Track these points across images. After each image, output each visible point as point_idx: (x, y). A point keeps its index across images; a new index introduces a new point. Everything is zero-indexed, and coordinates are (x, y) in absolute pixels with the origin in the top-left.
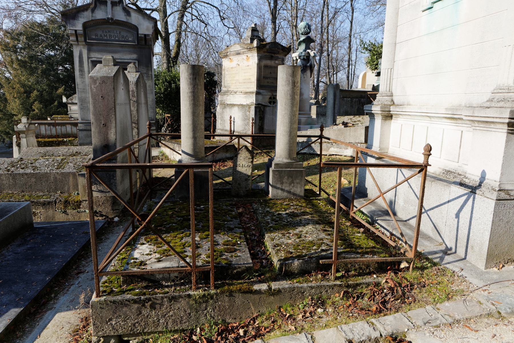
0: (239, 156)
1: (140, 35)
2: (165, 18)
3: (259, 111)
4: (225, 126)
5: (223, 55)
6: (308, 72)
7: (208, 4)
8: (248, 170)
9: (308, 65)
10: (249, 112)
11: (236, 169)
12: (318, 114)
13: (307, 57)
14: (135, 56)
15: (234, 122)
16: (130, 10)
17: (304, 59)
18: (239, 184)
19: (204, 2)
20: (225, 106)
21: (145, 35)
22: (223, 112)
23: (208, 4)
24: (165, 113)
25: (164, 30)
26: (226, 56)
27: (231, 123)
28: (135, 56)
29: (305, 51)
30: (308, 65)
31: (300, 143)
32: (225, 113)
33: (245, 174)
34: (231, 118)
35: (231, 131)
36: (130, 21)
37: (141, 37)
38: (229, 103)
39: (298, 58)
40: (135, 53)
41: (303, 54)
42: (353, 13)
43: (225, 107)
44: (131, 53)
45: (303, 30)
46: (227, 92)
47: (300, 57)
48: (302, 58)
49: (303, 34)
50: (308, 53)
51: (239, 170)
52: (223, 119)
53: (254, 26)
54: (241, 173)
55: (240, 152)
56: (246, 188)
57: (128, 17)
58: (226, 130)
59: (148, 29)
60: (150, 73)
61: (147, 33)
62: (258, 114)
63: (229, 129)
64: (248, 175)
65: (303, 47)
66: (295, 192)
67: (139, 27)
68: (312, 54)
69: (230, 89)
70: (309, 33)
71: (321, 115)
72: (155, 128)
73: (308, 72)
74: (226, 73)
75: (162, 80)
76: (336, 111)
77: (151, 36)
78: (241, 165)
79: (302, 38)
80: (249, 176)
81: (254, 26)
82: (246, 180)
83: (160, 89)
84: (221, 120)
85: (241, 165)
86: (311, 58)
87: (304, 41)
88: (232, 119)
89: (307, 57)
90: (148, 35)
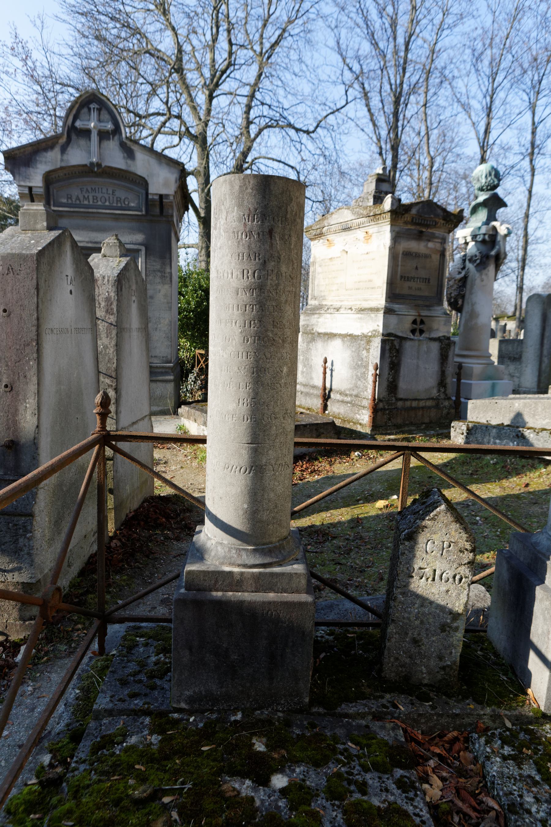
0: (422, 538)
1: (150, 197)
2: (206, 186)
3: (390, 349)
4: (312, 378)
5: (314, 233)
6: (491, 268)
7: (280, 161)
9: (493, 253)
10: (368, 350)
11: (407, 585)
12: (501, 357)
13: (490, 236)
14: (139, 237)
15: (332, 370)
16: (135, 148)
17: (484, 242)
18: (416, 642)
19: (273, 160)
20: (315, 336)
21: (161, 196)
22: (308, 350)
23: (280, 161)
24: (195, 348)
25: (203, 206)
26: (320, 235)
27: (325, 373)
28: (139, 237)
29: (487, 223)
30: (493, 253)
31: (494, 427)
32: (313, 352)
33: (442, 608)
34: (325, 361)
35: (325, 388)
36: (132, 169)
37: (153, 200)
38: (321, 330)
39: (469, 239)
40: (140, 231)
41: (483, 230)
42: (533, 175)
43: (313, 340)
44: (133, 230)
45: (483, 181)
46: (320, 307)
47: (474, 237)
48: (480, 238)
49: (481, 189)
50: (494, 228)
51: (420, 591)
52: (309, 366)
53: (381, 172)
54: (424, 601)
55: (426, 522)
56: (441, 658)
57: (129, 162)
58: (314, 387)
59: (166, 184)
60: (168, 270)
61: (163, 192)
62: (387, 355)
63: (320, 384)
64: (451, 612)
65: (482, 215)
67: (150, 181)
68: (502, 230)
69: (324, 303)
70: (495, 187)
71: (510, 358)
72: (172, 377)
73: (491, 268)
74: (319, 269)
75: (194, 285)
76: (545, 352)
77: (172, 198)
78: (428, 571)
79: (483, 197)
80: (456, 616)
81: (381, 172)
82: (444, 628)
83: (188, 303)
84: (305, 366)
85: (428, 571)
86: (499, 238)
87: (485, 204)
88: (329, 364)
89: (490, 236)
90: (167, 196)
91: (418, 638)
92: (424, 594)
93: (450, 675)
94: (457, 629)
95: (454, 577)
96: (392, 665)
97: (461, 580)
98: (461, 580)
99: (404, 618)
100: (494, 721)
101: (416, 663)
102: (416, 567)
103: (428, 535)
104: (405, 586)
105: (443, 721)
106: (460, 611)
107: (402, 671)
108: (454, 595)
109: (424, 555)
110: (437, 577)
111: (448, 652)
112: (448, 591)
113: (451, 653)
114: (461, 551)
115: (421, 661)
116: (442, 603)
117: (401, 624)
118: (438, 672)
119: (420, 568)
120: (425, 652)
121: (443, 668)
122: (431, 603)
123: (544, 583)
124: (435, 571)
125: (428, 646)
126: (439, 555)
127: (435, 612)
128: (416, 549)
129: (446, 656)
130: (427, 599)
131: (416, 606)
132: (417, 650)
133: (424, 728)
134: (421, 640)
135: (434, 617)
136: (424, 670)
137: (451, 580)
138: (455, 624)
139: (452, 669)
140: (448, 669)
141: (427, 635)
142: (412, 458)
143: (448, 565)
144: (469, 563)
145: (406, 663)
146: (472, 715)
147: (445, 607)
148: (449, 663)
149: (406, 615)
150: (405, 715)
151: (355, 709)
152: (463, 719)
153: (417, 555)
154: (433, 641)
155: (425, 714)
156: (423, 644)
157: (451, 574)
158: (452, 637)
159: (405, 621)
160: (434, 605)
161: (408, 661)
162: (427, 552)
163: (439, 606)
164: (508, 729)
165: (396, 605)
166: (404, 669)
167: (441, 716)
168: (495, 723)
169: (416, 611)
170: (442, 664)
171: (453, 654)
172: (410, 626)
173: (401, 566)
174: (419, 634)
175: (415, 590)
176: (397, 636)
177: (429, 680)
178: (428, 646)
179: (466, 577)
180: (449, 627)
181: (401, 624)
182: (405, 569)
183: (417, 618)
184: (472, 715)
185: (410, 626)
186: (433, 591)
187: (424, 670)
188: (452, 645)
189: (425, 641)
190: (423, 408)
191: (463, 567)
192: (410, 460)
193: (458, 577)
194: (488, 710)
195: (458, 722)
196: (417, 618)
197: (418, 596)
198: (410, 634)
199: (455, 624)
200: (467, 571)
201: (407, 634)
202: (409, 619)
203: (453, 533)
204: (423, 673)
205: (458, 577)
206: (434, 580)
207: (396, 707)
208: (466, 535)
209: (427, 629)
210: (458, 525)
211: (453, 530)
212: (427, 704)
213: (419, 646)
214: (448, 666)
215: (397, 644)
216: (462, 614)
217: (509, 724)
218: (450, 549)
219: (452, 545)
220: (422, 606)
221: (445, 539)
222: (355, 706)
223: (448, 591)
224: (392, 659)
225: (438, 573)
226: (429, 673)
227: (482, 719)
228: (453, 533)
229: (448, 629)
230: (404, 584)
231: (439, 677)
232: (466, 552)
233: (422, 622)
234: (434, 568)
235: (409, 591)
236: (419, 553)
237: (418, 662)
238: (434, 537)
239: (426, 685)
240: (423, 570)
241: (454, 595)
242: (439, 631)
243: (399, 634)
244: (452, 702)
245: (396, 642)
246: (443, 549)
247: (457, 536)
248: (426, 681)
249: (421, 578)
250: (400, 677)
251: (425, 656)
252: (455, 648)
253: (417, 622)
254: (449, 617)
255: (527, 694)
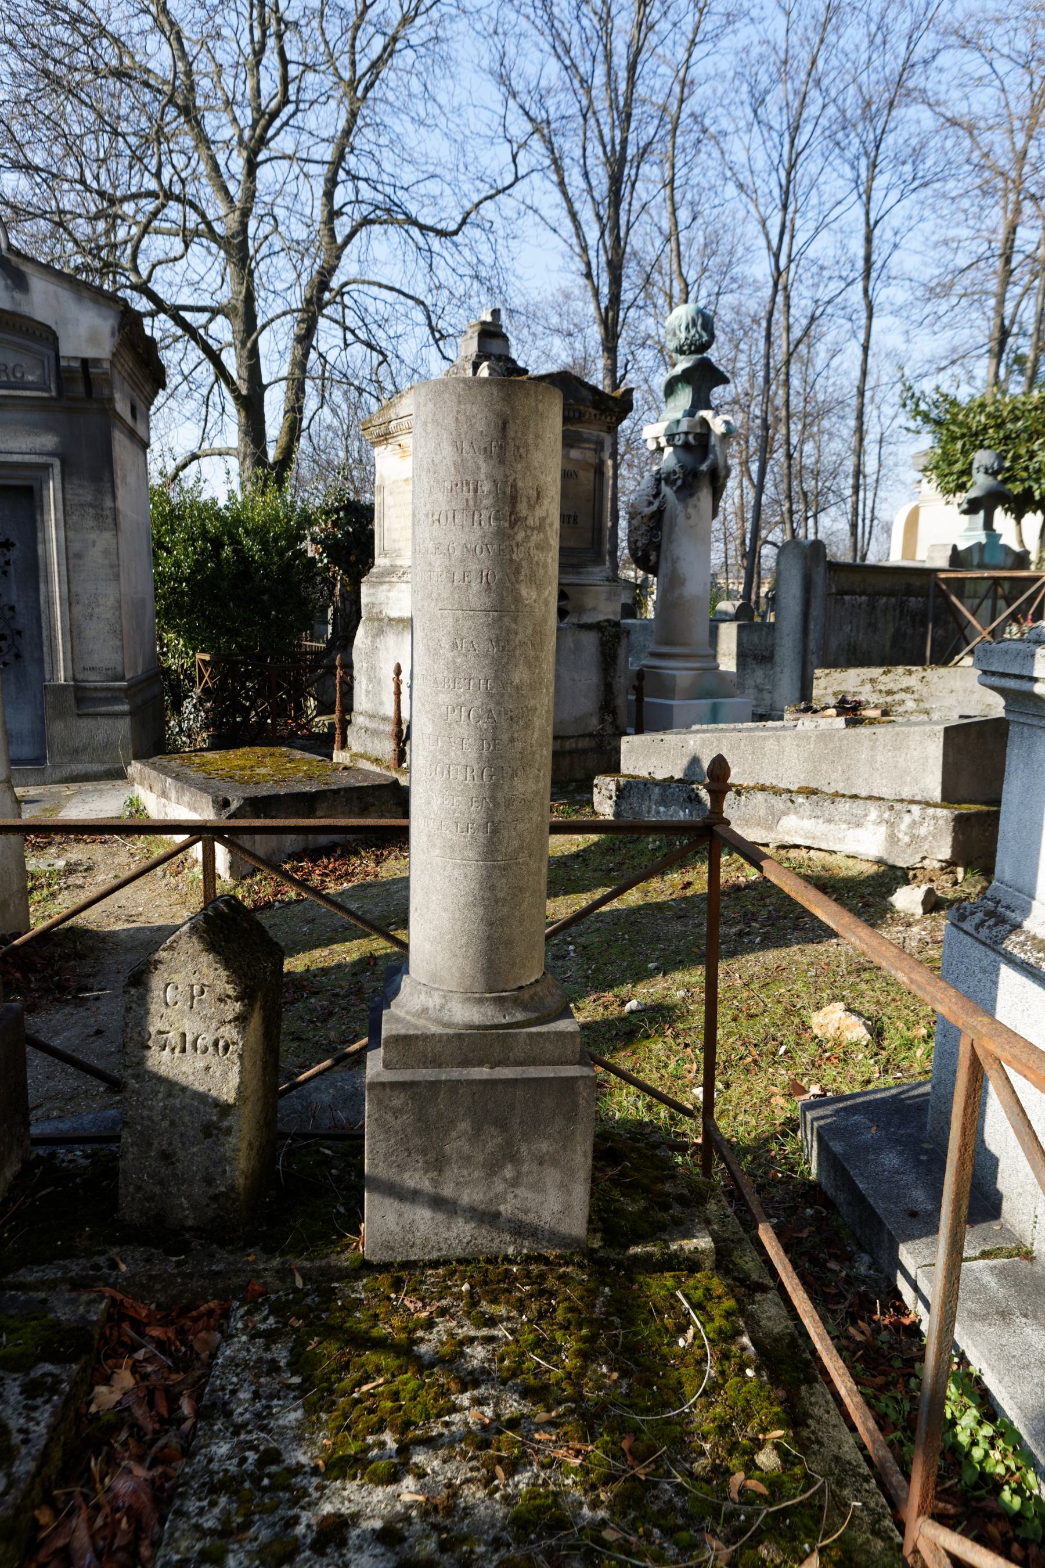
0: (157, 981)
1: (63, 363)
2: (249, 336)
4: (381, 703)
5: (376, 431)
6: (705, 496)
7: (392, 289)
8: (217, 1071)
9: (704, 467)
11: (142, 1061)
12: (743, 656)
13: (697, 436)
14: (48, 441)
15: (411, 687)
16: (27, 268)
17: (686, 446)
18: (166, 1157)
19: (380, 285)
20: (387, 624)
21: (85, 362)
22: (375, 649)
23: (392, 289)
24: (194, 650)
25: (245, 374)
26: (385, 437)
27: (398, 693)
28: (48, 441)
29: (691, 413)
30: (704, 467)
31: (656, 783)
32: (382, 654)
33: (202, 1098)
34: (398, 671)
35: (399, 721)
36: (25, 310)
37: (69, 369)
38: (394, 614)
39: (663, 442)
40: (49, 428)
41: (684, 427)
42: (870, 317)
43: (381, 632)
44: (34, 428)
45: (683, 335)
46: (391, 571)
47: (671, 437)
48: (679, 441)
49: (680, 351)
50: (704, 422)
51: (163, 1071)
52: (374, 678)
53: (489, 319)
54: (172, 1087)
55: (162, 955)
56: (209, 1181)
57: (18, 296)
58: (385, 719)
59: (93, 339)
60: (108, 503)
61: (90, 353)
63: (390, 711)
64: (216, 1103)
65: (684, 397)
66: (530, 1218)
67: (60, 333)
68: (718, 426)
69: (399, 563)
70: (704, 347)
71: (755, 657)
72: (126, 708)
73: (705, 496)
74: (389, 500)
75: (187, 530)
76: (812, 645)
77: (106, 365)
78: (173, 1037)
79: (684, 364)
80: (224, 1109)
81: (489, 319)
82: (209, 1130)
83: (177, 564)
84: (370, 680)
85: (173, 1037)
86: (713, 440)
87: (686, 377)
88: (405, 677)
89: (697, 436)
90: (97, 361)
94: (229, 1131)
95: (216, 1044)
97: (226, 1048)
98: (226, 1048)
102: (153, 1030)
106: (231, 1101)
109: (163, 1010)
110: (188, 1046)
114: (221, 1000)
116: (201, 1089)
119: (161, 1033)
121: (215, 1198)
122: (184, 1089)
124: (184, 1035)
126: (186, 1008)
130: (176, 1084)
135: (191, 1114)
137: (211, 1049)
138: (226, 1124)
144: (236, 1019)
149: (146, 1113)
150: (126, 1279)
159: (147, 1123)
161: (157, 1189)
167: (190, 1276)
170: (212, 1191)
174: (170, 1144)
175: (155, 1069)
176: (135, 1149)
182: (136, 1036)
183: (164, 1117)
188: (224, 1159)
189: (181, 1154)
190: (571, 752)
193: (221, 1043)
195: (220, 1286)
196: (164, 1117)
199: (226, 1124)
200: (234, 1033)
201: (150, 1145)
202: (150, 1118)
203: (205, 970)
209: (182, 1135)
214: (222, 1194)
223: (207, 1068)
224: (131, 1189)
225: (189, 1038)
228: (205, 970)
233: (172, 1123)
236: (155, 1007)
237: (174, 1190)
238: (176, 978)
239: (190, 1229)
247: (212, 974)
248: (190, 1222)
253: (165, 1124)
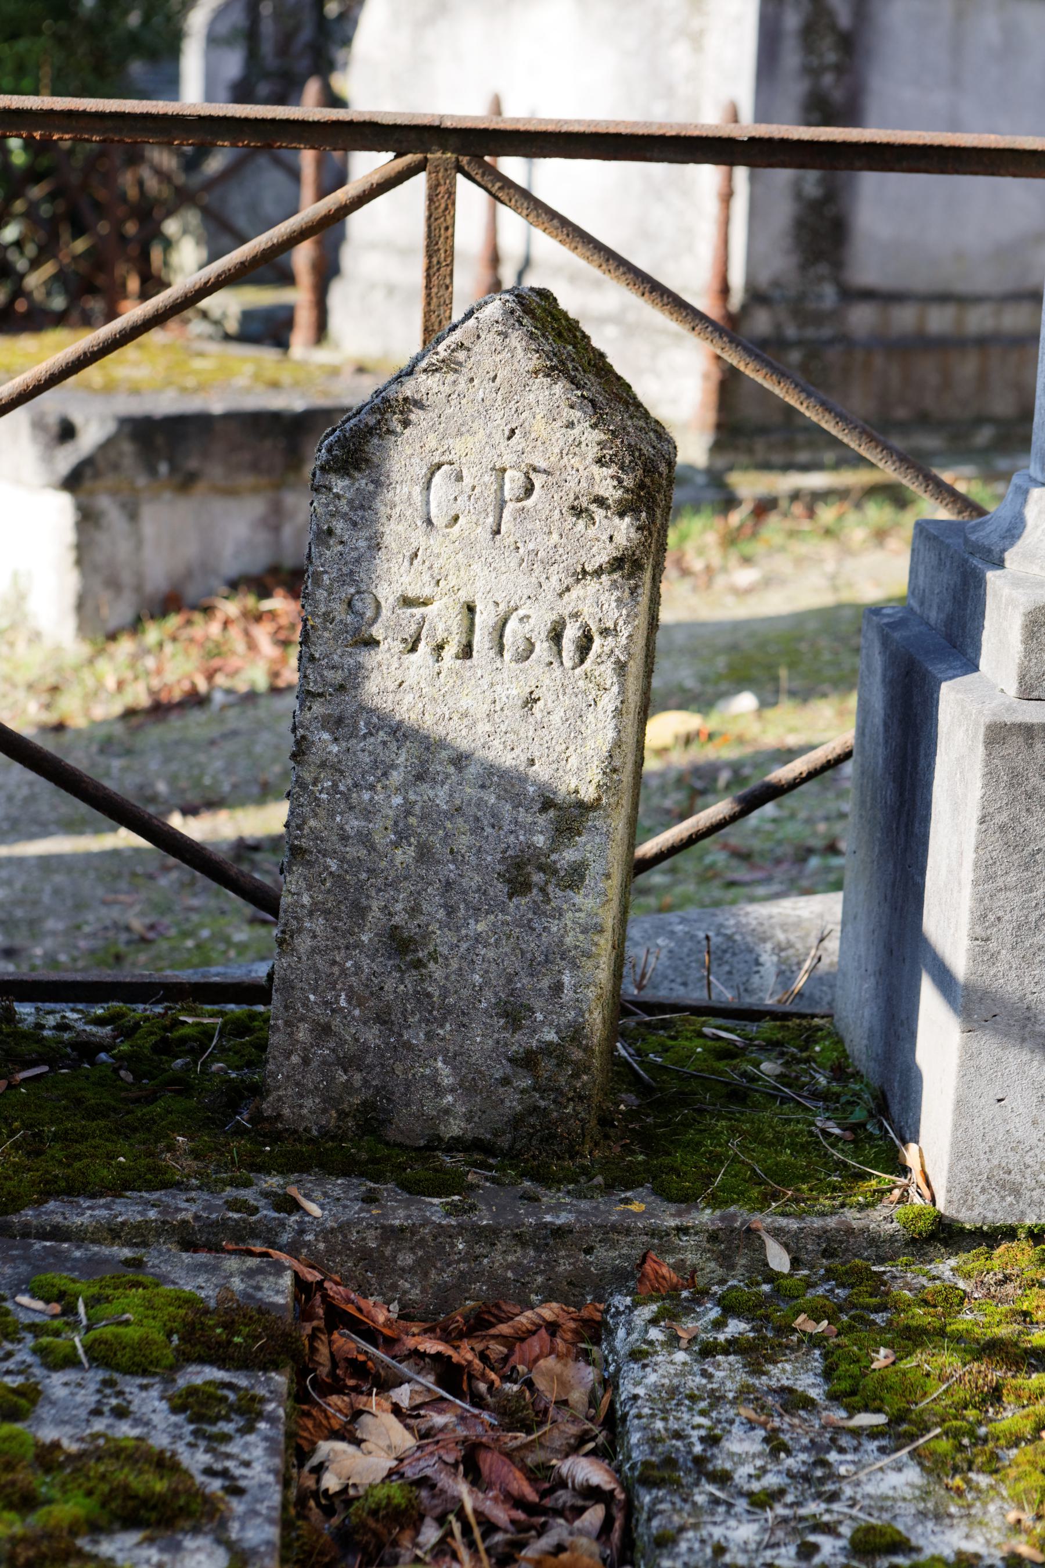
3: (809, 33)
8: (555, 709)
10: (696, 40)
18: (401, 945)
33: (507, 783)
51: (407, 709)
54: (430, 755)
56: (514, 1014)
62: (791, 58)
80: (570, 817)
82: (520, 874)
85: (442, 618)
91: (412, 928)
92: (429, 720)
93: (558, 1090)
94: (575, 877)
95: (556, 636)
96: (306, 1061)
97: (584, 647)
98: (584, 647)
99: (344, 838)
100: (726, 1261)
101: (408, 1046)
102: (387, 594)
103: (432, 441)
104: (341, 688)
105: (501, 1259)
106: (588, 793)
107: (348, 1086)
108: (556, 718)
109: (419, 538)
110: (481, 641)
111: (545, 983)
112: (530, 701)
113: (558, 988)
114: (578, 511)
115: (430, 1036)
116: (508, 760)
117: (333, 865)
118: (506, 1081)
119: (407, 602)
120: (445, 994)
121: (527, 1061)
122: (460, 760)
123: (976, 668)
124: (471, 609)
125: (454, 965)
126: (483, 533)
127: (480, 803)
128: (383, 510)
129: (538, 1004)
130: (441, 744)
131: (396, 777)
132: (408, 986)
133: (415, 1294)
134: (427, 935)
135: (477, 829)
136: (446, 1076)
137: (543, 648)
138: (569, 856)
139: (563, 1061)
140: (547, 1065)
141: (451, 911)
142: (462, 183)
143: (523, 580)
144: (617, 563)
145: (366, 1049)
146: (628, 1232)
147: (523, 779)
148: (551, 1036)
149: (354, 824)
150: (326, 1234)
151: (105, 1213)
152: (589, 1251)
153: (388, 540)
154: (478, 938)
155: (413, 1230)
156: (433, 957)
157: (540, 622)
158: (560, 913)
159: (355, 851)
160: (472, 770)
161: (371, 1035)
162: (429, 522)
163: (495, 777)
164: (772, 1277)
165: (308, 777)
166: (358, 1077)
167: (488, 1236)
168: (732, 1267)
169: (397, 800)
170: (519, 1042)
171: (567, 995)
172: (371, 872)
173: (321, 594)
174: (414, 911)
176: (318, 924)
177: (469, 1118)
178: (454, 965)
179: (605, 632)
180: (541, 868)
181: (333, 865)
182: (339, 610)
183: (402, 837)
184: (628, 1232)
185: (371, 872)
186: (465, 702)
187: (446, 1076)
188: (558, 954)
189: (442, 939)
190: (983, 342)
191: (592, 586)
192: (451, 194)
193: (571, 633)
194: (705, 1217)
195: (564, 1267)
196: (402, 837)
197: (400, 733)
198: (375, 913)
199: (569, 856)
200: (609, 600)
201: (360, 911)
202: (365, 839)
203: (539, 427)
204: (440, 1091)
205: (571, 633)
206: (467, 651)
207: (292, 1206)
208: (597, 435)
209: (448, 885)
210: (559, 388)
211: (541, 411)
212: (436, 1201)
213: (419, 964)
214: (547, 1049)
215: (320, 962)
216: (594, 806)
217: (779, 1259)
218: (529, 503)
219: (538, 480)
220: (420, 777)
221: (508, 459)
222: (107, 1207)
223: (530, 701)
224: (303, 1034)
225: (484, 619)
226: (467, 1087)
227: (672, 1250)
228: (539, 427)
229: (537, 878)
230: (335, 677)
231: (513, 1103)
232: (599, 513)
233: (424, 854)
234: (463, 596)
235: (362, 708)
236: (397, 530)
237: (417, 1037)
238: (458, 447)
239: (456, 1145)
240: (418, 611)
241: (556, 718)
242: (500, 889)
243: (327, 912)
244: (548, 1197)
245: (314, 950)
246: (501, 505)
247: (559, 438)
248: (455, 1128)
249: (413, 649)
250: (342, 1115)
251: (447, 1012)
252: (575, 966)
253: (405, 855)
254: (542, 820)
255: (904, 1170)
